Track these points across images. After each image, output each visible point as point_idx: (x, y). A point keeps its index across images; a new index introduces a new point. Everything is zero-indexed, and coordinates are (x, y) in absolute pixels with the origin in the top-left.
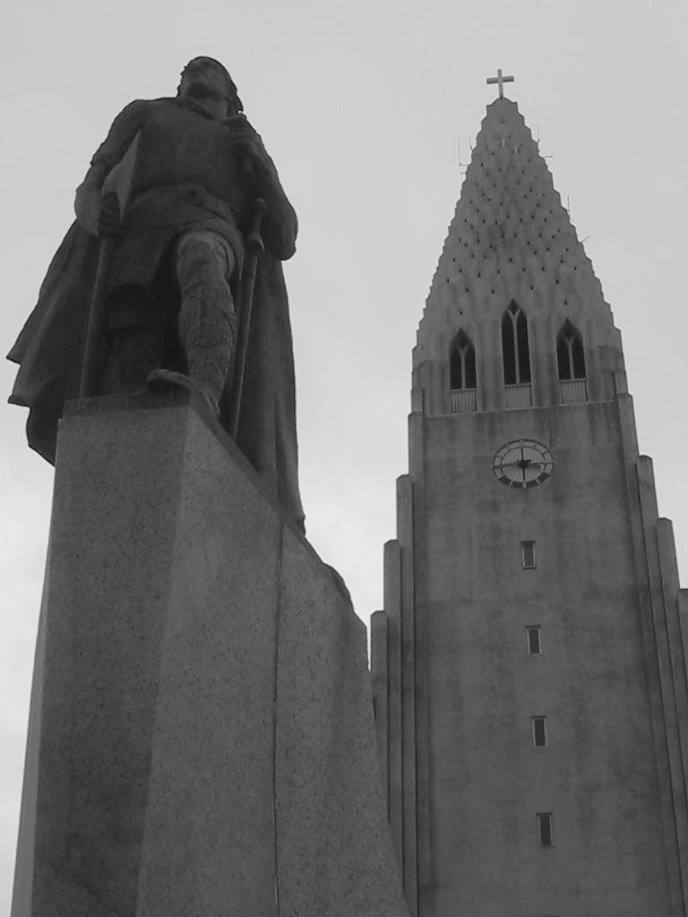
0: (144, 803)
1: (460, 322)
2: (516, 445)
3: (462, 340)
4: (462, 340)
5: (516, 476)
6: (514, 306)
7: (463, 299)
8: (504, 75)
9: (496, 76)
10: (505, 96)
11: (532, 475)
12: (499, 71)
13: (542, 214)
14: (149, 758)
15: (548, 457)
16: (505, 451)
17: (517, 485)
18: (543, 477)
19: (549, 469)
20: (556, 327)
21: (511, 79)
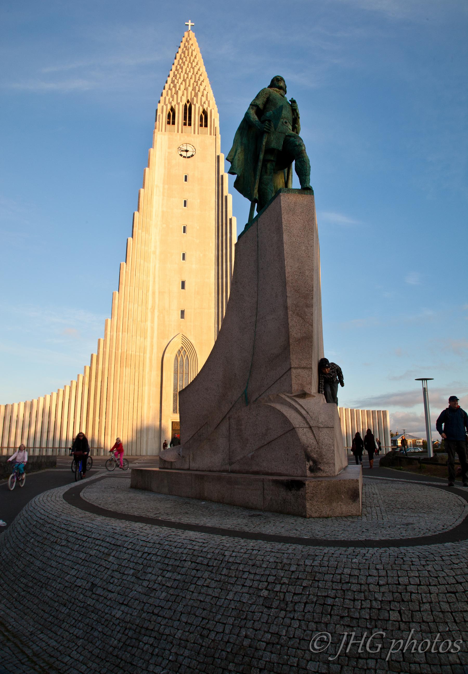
0: (313, 298)
3: (172, 110)
4: (172, 110)
5: (184, 154)
6: (188, 102)
11: (189, 154)
14: (313, 287)
15: (194, 150)
17: (184, 157)
18: (192, 156)
19: (194, 154)
20: (201, 110)
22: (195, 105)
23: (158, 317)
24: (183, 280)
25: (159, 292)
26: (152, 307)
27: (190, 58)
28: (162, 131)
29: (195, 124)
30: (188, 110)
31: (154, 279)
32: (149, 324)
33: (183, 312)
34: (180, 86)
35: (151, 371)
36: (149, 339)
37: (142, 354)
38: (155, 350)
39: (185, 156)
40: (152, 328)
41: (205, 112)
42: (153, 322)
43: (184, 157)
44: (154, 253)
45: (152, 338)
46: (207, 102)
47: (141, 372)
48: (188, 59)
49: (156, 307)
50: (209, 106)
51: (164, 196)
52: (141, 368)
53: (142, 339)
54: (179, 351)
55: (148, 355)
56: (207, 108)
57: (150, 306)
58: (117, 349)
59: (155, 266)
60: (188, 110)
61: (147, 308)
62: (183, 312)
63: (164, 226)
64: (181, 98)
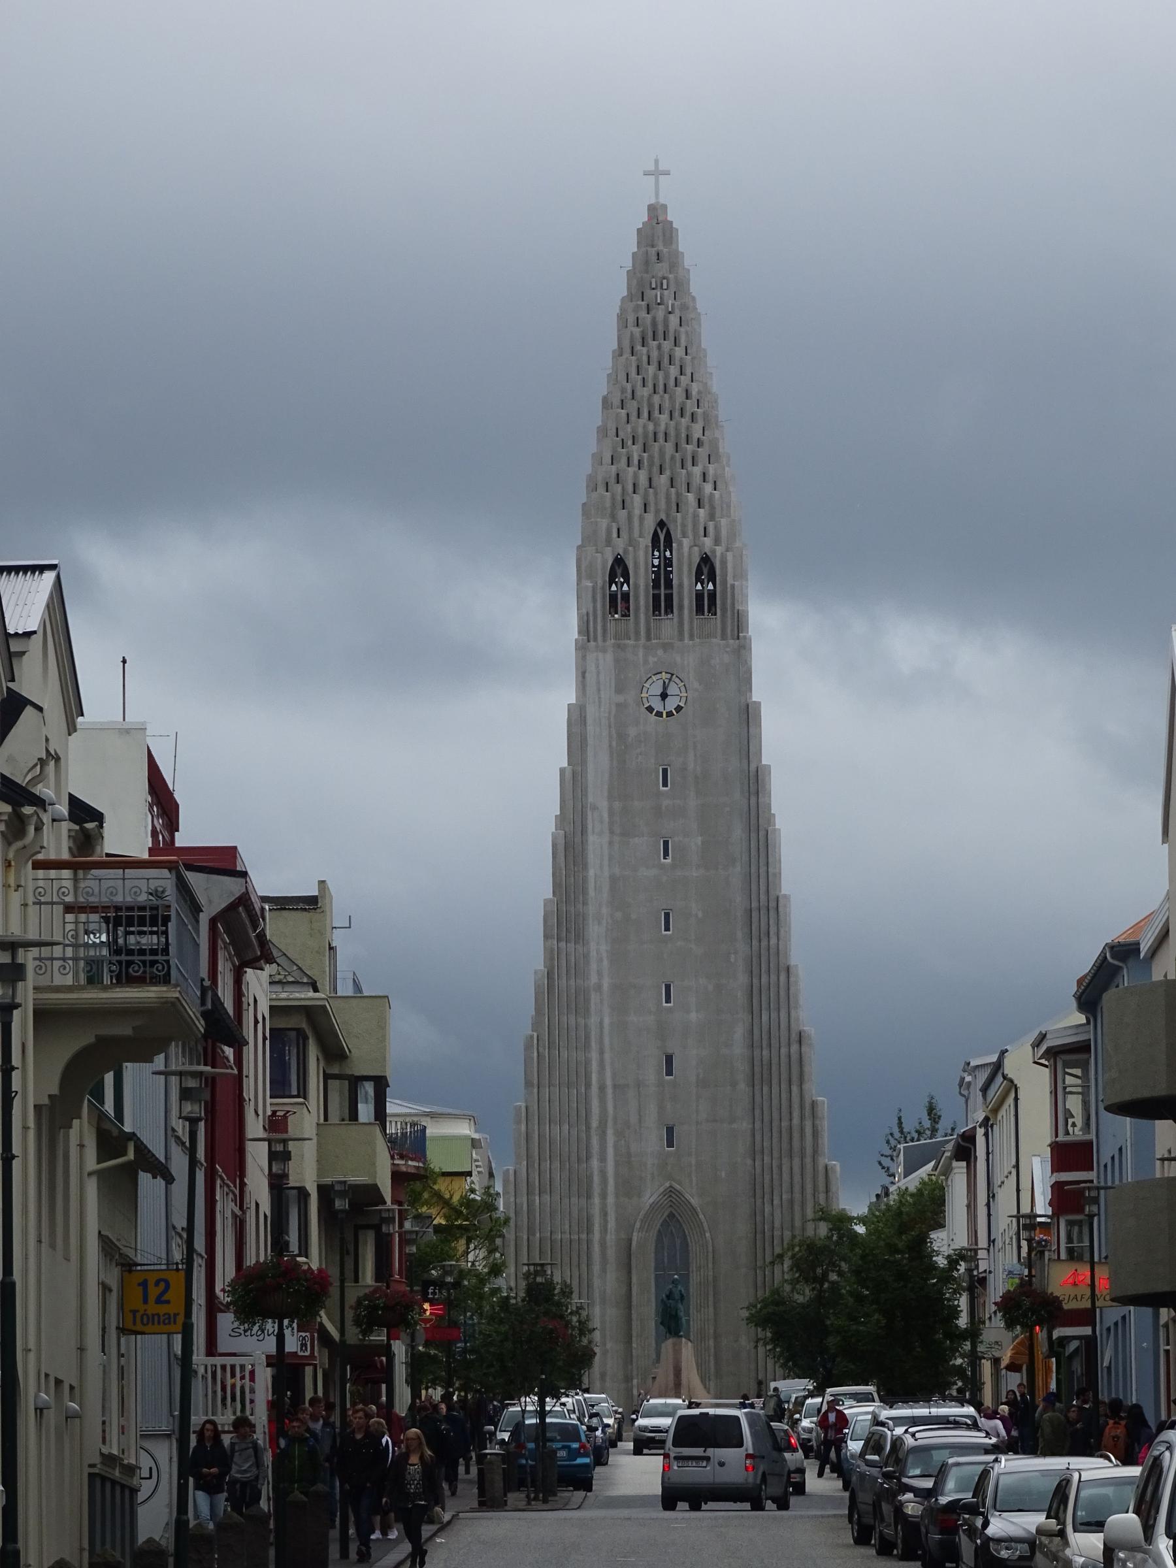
1: (620, 545)
2: (659, 676)
6: (661, 524)
7: (622, 514)
8: (660, 169)
9: (653, 168)
10: (662, 201)
11: (671, 703)
12: (657, 162)
13: (690, 406)
15: (683, 689)
16: (650, 681)
17: (659, 714)
18: (679, 709)
19: (682, 704)
20: (696, 560)
21: (667, 173)
22: (680, 545)
23: (615, 1147)
24: (670, 1051)
25: (615, 1087)
26: (600, 1123)
27: (659, 347)
28: (595, 640)
29: (681, 607)
30: (662, 578)
31: (601, 1052)
32: (595, 1163)
33: (670, 1131)
34: (636, 476)
35: (604, 1270)
36: (596, 1200)
37: (584, 1236)
38: (612, 1225)
39: (661, 710)
40: (603, 1173)
41: (706, 560)
42: (603, 1159)
43: (659, 714)
44: (599, 988)
45: (604, 1196)
46: (711, 530)
47: (585, 1275)
48: (655, 354)
49: (610, 1123)
50: (717, 541)
51: (612, 832)
52: (584, 1267)
53: (583, 1201)
54: (665, 1224)
55: (596, 1236)
56: (714, 552)
57: (594, 1124)
58: (531, 1231)
59: (601, 1023)
60: (662, 578)
61: (588, 1128)
62: (670, 1131)
63: (619, 915)
64: (641, 519)
